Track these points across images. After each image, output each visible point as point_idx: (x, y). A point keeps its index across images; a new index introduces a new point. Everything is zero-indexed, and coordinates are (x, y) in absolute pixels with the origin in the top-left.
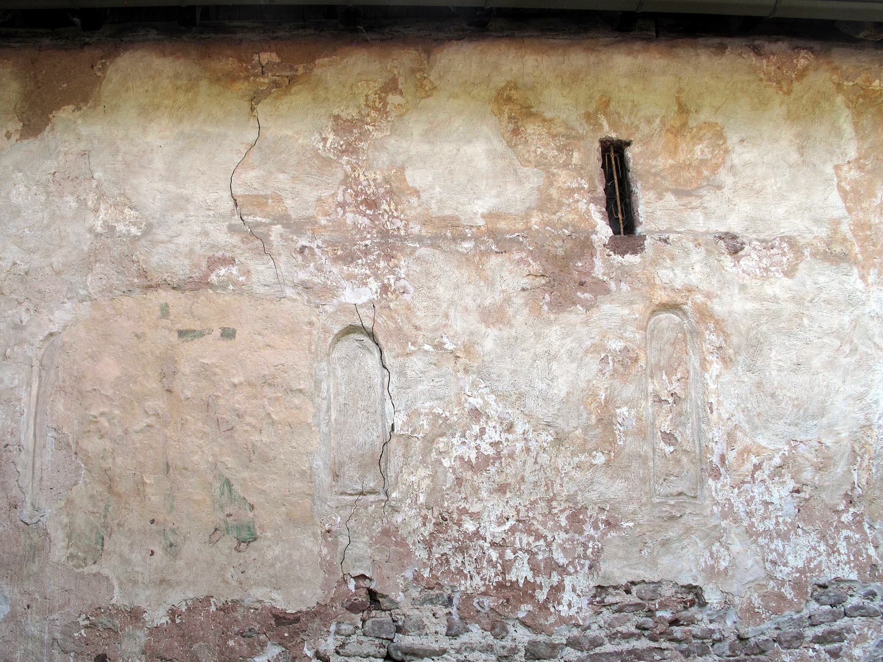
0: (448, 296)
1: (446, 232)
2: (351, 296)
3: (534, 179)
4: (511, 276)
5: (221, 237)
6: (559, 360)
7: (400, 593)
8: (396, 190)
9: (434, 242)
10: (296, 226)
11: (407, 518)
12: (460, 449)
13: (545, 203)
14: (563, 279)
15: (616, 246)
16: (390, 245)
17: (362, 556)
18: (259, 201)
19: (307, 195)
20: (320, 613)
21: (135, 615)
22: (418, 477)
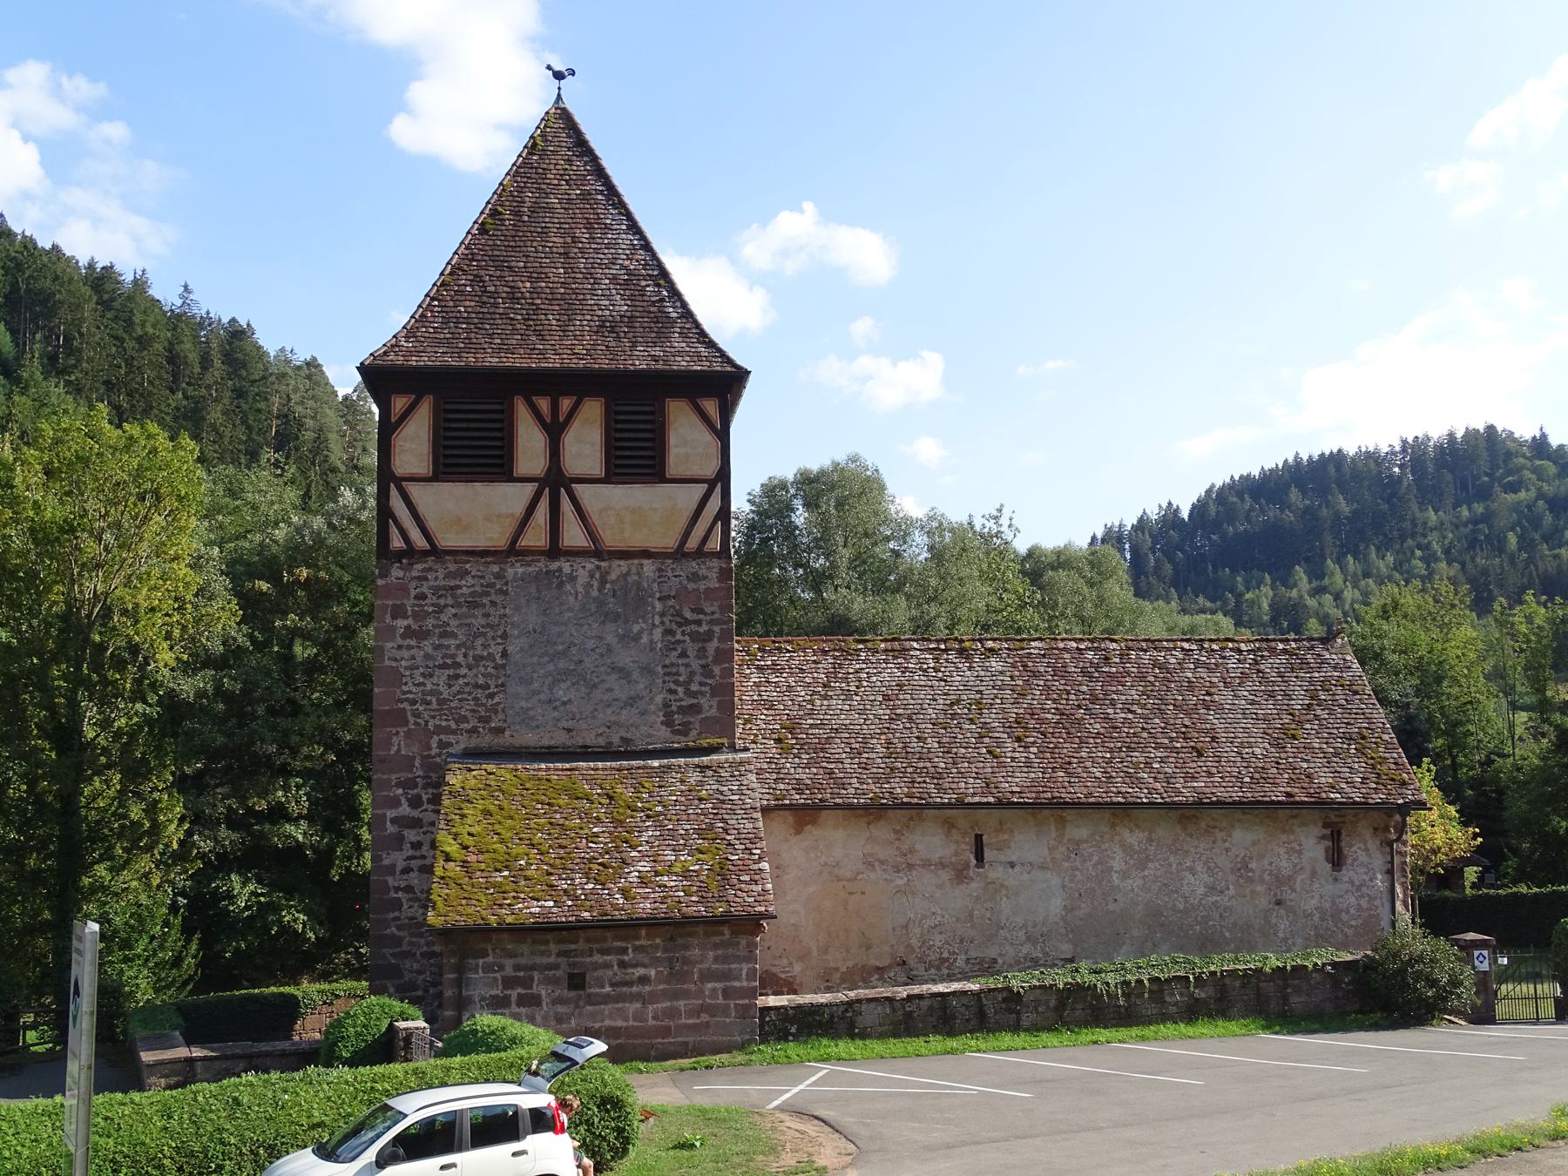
0: (927, 881)
1: (927, 864)
2: (899, 882)
3: (953, 847)
4: (945, 876)
5: (861, 867)
6: (959, 898)
7: (912, 962)
8: (912, 851)
9: (923, 866)
10: (882, 862)
11: (915, 942)
12: (929, 922)
13: (956, 854)
14: (960, 875)
15: (977, 866)
16: (910, 866)
17: (901, 951)
18: (871, 855)
19: (885, 853)
20: (890, 967)
21: (837, 969)
22: (917, 931)
